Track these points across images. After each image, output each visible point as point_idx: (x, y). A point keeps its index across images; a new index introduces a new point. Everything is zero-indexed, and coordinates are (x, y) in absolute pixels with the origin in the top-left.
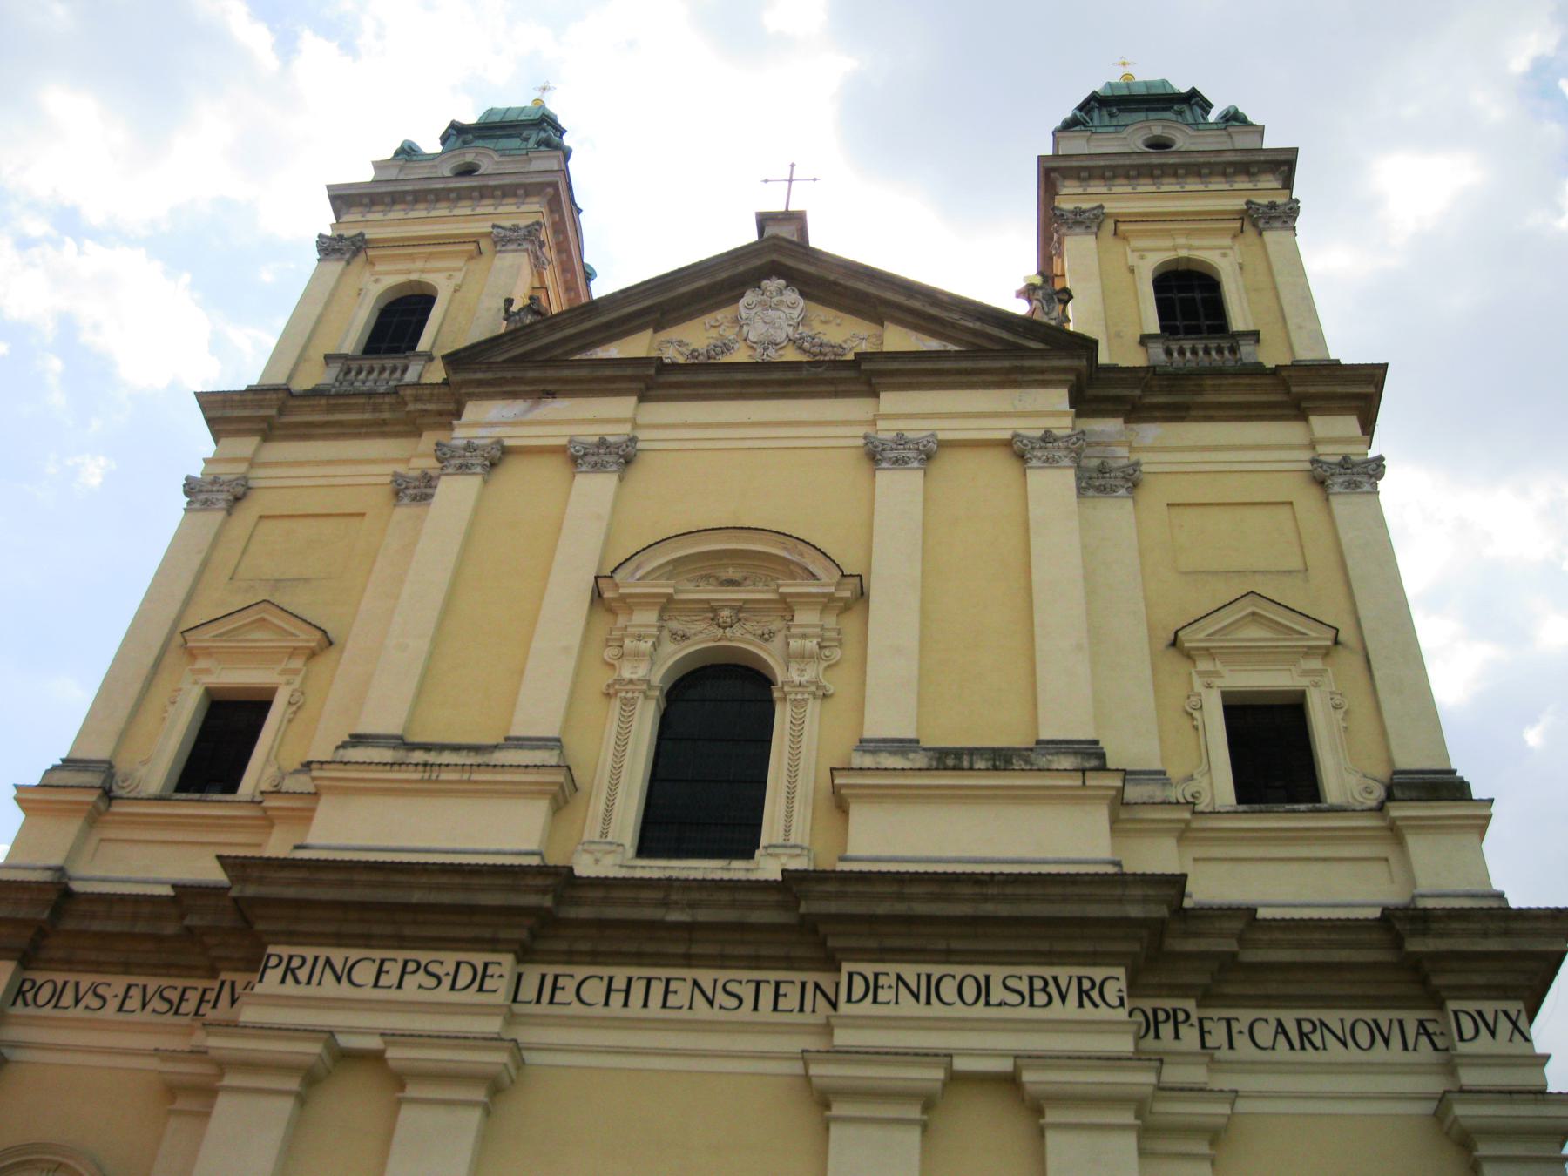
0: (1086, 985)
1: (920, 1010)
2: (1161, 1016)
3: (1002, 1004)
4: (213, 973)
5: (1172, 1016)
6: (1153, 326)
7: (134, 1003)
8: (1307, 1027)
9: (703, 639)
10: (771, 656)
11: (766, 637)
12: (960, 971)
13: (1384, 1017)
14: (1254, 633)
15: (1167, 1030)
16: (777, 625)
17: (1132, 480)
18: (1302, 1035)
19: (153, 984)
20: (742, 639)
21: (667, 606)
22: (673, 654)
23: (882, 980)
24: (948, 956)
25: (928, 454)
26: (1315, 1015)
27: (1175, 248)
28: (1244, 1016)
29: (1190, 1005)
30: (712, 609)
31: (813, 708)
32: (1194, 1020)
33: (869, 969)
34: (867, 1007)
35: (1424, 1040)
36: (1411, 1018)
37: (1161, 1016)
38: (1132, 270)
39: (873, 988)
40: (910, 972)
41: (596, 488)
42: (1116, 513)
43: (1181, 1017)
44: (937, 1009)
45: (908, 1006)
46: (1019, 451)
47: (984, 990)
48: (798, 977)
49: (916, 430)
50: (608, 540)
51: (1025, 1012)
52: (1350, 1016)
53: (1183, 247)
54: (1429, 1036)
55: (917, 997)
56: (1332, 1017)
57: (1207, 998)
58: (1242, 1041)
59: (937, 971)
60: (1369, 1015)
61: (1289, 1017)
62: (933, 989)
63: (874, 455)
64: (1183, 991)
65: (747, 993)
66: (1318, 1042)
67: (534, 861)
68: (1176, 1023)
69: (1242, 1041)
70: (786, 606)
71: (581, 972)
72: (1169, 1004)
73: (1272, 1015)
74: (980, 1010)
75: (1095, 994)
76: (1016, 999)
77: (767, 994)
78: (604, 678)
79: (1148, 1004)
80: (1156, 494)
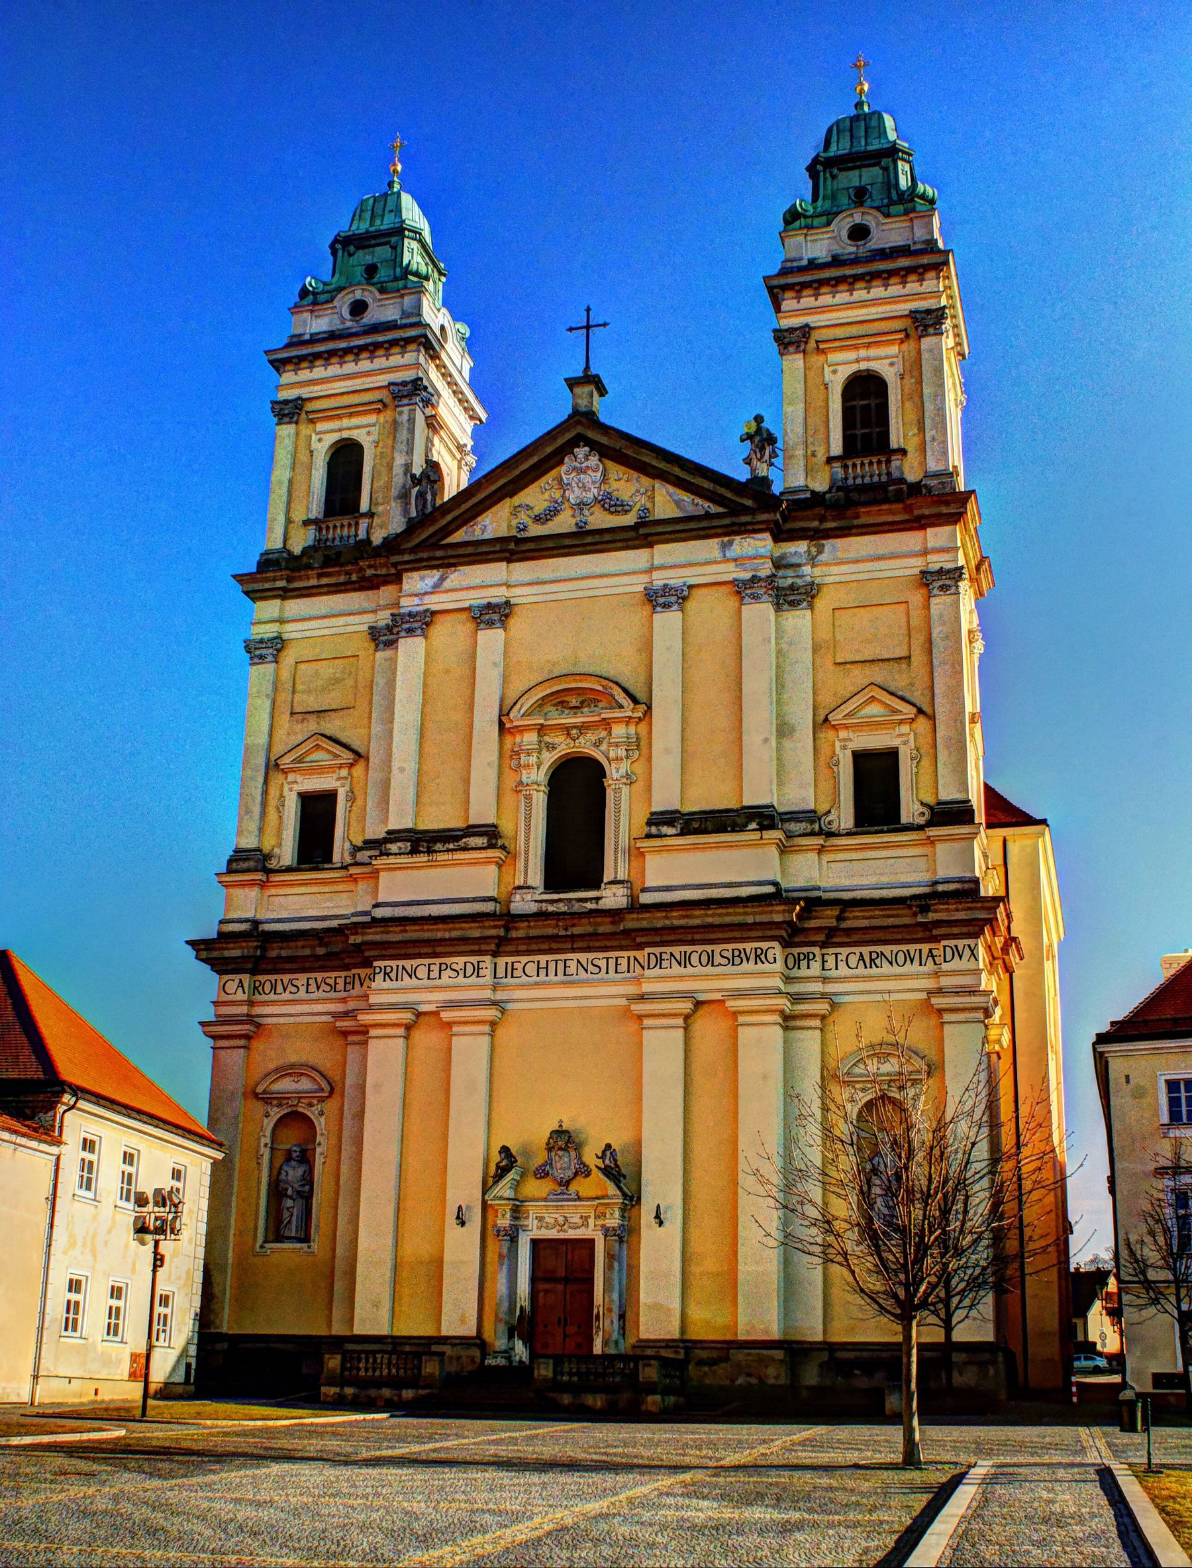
0: (759, 952)
1: (681, 970)
2: (802, 957)
3: (720, 964)
5: (807, 956)
8: (874, 956)
9: (564, 747)
11: (597, 744)
13: (912, 948)
15: (804, 964)
16: (604, 734)
18: (872, 960)
21: (541, 729)
22: (549, 758)
23: (664, 956)
26: (878, 949)
27: (858, 361)
28: (844, 951)
29: (816, 950)
30: (567, 729)
32: (818, 958)
34: (656, 972)
35: (930, 959)
36: (925, 948)
37: (802, 957)
38: (826, 386)
43: (811, 956)
44: (689, 970)
45: (677, 970)
48: (625, 954)
49: (675, 578)
52: (895, 948)
53: (864, 359)
54: (933, 957)
55: (680, 964)
56: (886, 949)
57: (823, 945)
58: (842, 965)
60: (905, 947)
61: (866, 950)
65: (603, 963)
66: (879, 964)
68: (809, 960)
69: (842, 965)
70: (607, 724)
72: (805, 950)
73: (857, 950)
75: (763, 957)
76: (726, 961)
77: (612, 962)
79: (795, 951)
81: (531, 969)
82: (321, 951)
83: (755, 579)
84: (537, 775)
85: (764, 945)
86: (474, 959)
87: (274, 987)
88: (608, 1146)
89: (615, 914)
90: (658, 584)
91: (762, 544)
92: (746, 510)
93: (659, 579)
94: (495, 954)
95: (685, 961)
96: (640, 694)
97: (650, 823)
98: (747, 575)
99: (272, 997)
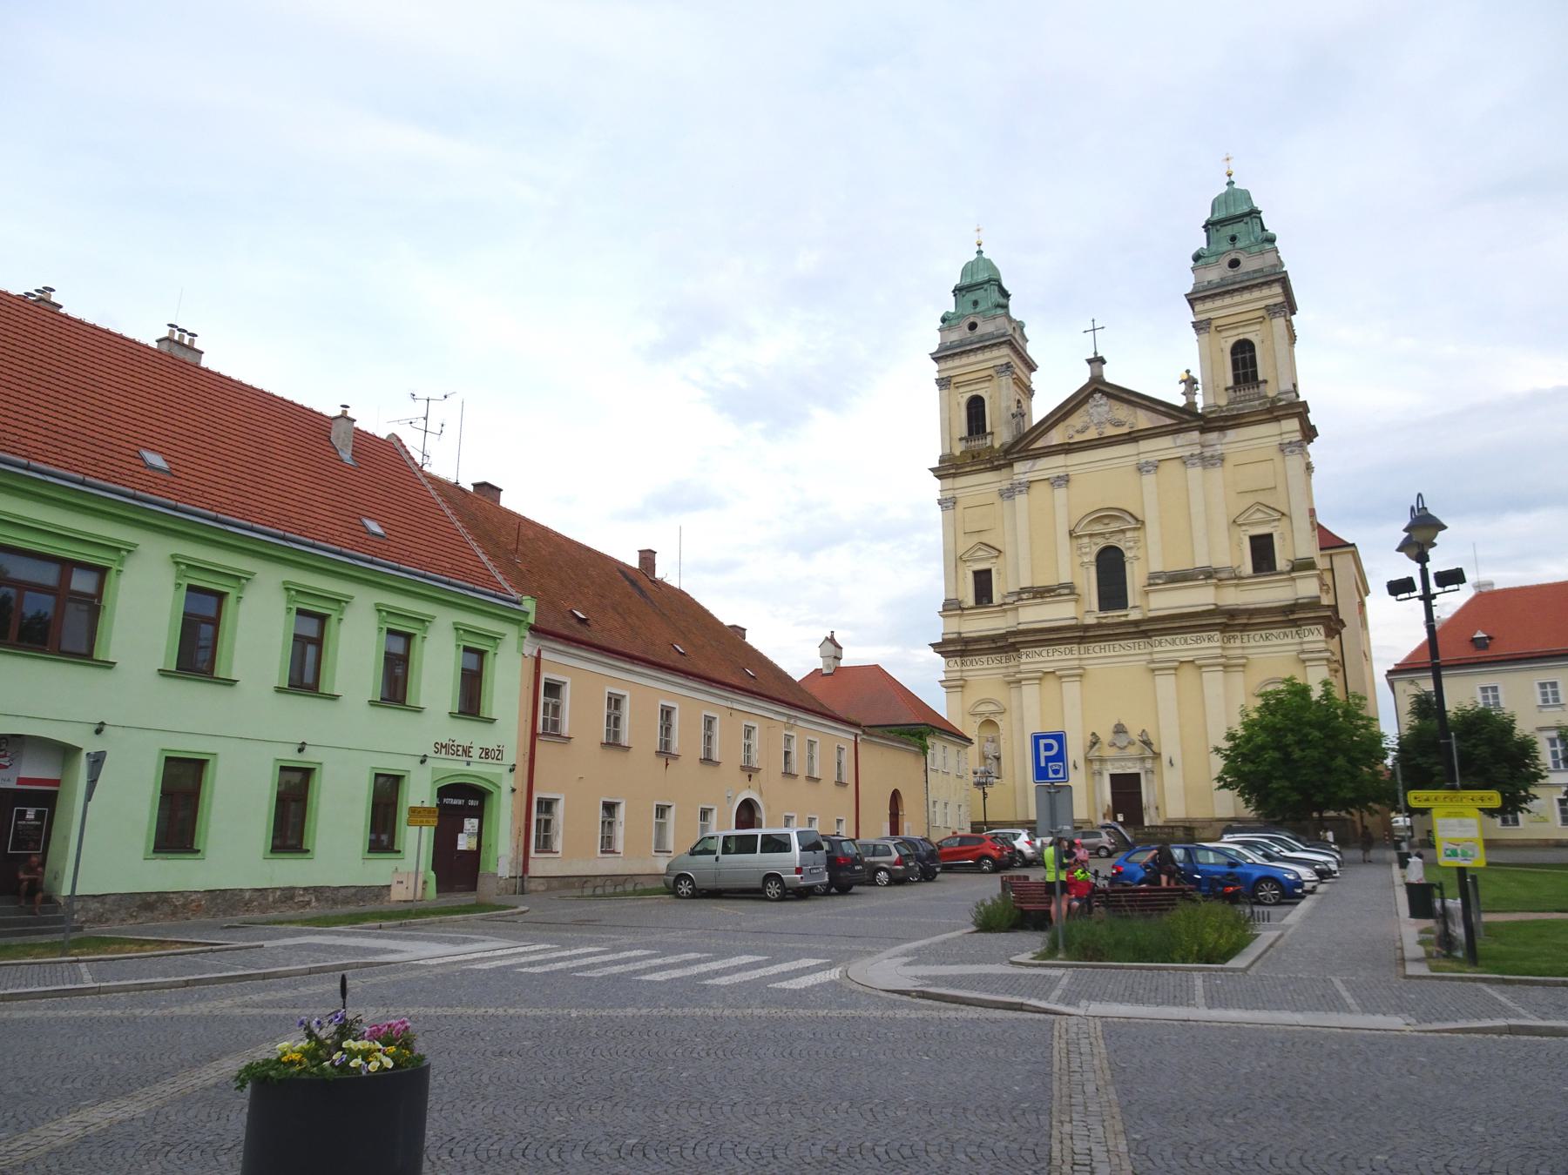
4: (1006, 652)
6: (1230, 383)
7: (990, 662)
9: (1102, 543)
10: (1121, 545)
12: (1179, 636)
14: (1259, 515)
17: (1222, 459)
19: (993, 656)
20: (1113, 541)
22: (1096, 549)
24: (1177, 634)
25: (1156, 466)
31: (1136, 563)
33: (1158, 638)
34: (1159, 649)
39: (1160, 643)
40: (1168, 638)
41: (1061, 493)
42: (1216, 474)
44: (1176, 648)
45: (1170, 648)
46: (1184, 461)
47: (1186, 641)
50: (1069, 521)
51: (1196, 646)
59: (1174, 637)
62: (1174, 641)
63: (1140, 469)
64: (1237, 631)
65: (1132, 645)
67: (1073, 622)
71: (1093, 645)
74: (1186, 647)
78: (1079, 561)
80: (1229, 464)
81: (1097, 649)
82: (993, 645)
83: (1192, 455)
84: (1091, 558)
85: (1212, 633)
86: (1069, 646)
87: (971, 662)
88: (1144, 731)
89: (1136, 623)
90: (1143, 461)
91: (1195, 435)
92: (1188, 422)
93: (1143, 459)
94: (1079, 643)
95: (1174, 642)
96: (1140, 518)
97: (1149, 578)
98: (1188, 454)
99: (971, 667)
